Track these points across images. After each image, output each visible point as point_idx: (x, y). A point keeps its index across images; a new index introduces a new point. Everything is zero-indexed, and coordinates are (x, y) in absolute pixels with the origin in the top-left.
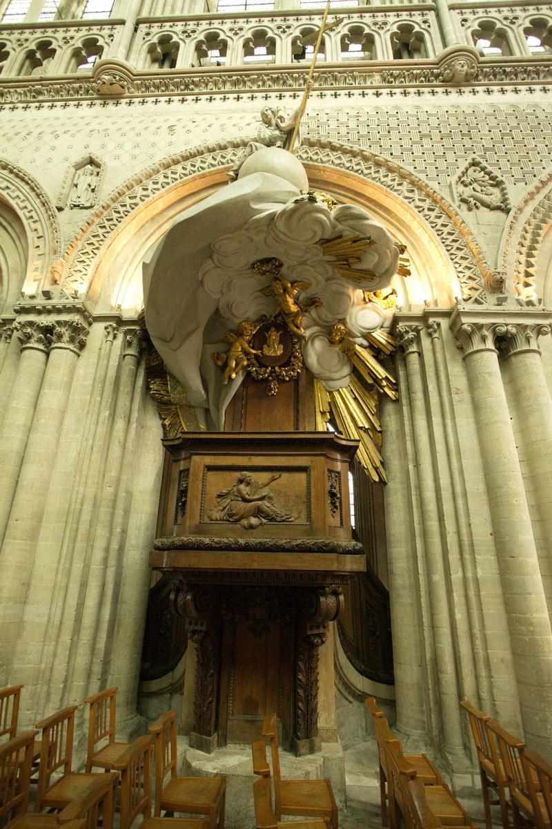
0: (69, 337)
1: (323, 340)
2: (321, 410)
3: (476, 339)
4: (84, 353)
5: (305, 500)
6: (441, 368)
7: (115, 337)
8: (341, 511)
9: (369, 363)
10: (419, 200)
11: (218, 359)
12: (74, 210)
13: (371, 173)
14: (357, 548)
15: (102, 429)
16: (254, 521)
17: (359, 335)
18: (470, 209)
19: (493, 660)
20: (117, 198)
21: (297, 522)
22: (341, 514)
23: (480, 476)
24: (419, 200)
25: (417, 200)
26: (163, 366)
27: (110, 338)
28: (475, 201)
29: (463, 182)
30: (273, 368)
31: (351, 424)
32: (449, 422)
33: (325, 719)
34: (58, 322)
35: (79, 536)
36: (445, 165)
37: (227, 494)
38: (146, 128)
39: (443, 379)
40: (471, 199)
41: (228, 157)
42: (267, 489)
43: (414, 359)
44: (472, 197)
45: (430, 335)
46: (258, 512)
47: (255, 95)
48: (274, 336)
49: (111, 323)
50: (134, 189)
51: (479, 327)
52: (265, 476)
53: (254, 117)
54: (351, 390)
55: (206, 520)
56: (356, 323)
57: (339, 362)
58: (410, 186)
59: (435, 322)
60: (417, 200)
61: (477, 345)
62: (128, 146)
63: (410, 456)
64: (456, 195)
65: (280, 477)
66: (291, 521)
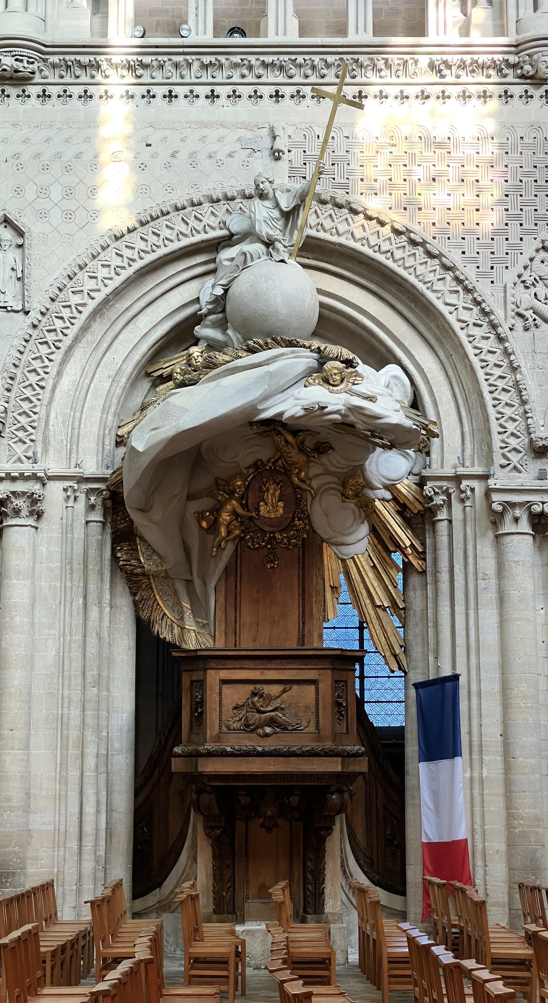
0: (29, 512)
2: (332, 584)
3: (508, 518)
4: (42, 525)
5: (313, 710)
6: (470, 548)
7: (75, 498)
8: (347, 718)
9: (391, 526)
10: (464, 308)
11: (203, 518)
13: (404, 258)
14: (360, 752)
15: (78, 620)
16: (268, 730)
17: (382, 487)
18: (526, 329)
19: (489, 852)
21: (307, 730)
22: (347, 721)
23: (497, 675)
24: (464, 308)
25: (461, 309)
26: (133, 528)
27: (71, 503)
28: (535, 316)
29: (523, 282)
31: (368, 601)
32: (472, 613)
33: (332, 905)
34: (13, 493)
35: (71, 743)
36: (505, 248)
37: (243, 706)
38: (78, 156)
39: (471, 560)
40: (529, 314)
41: (205, 220)
42: (279, 701)
43: (443, 527)
44: (531, 308)
45: (462, 501)
47: (240, 89)
49: (71, 483)
50: (77, 277)
51: (513, 505)
53: (239, 140)
55: (225, 729)
58: (454, 283)
60: (461, 309)
61: (508, 527)
62: (56, 193)
63: (431, 646)
64: (510, 306)
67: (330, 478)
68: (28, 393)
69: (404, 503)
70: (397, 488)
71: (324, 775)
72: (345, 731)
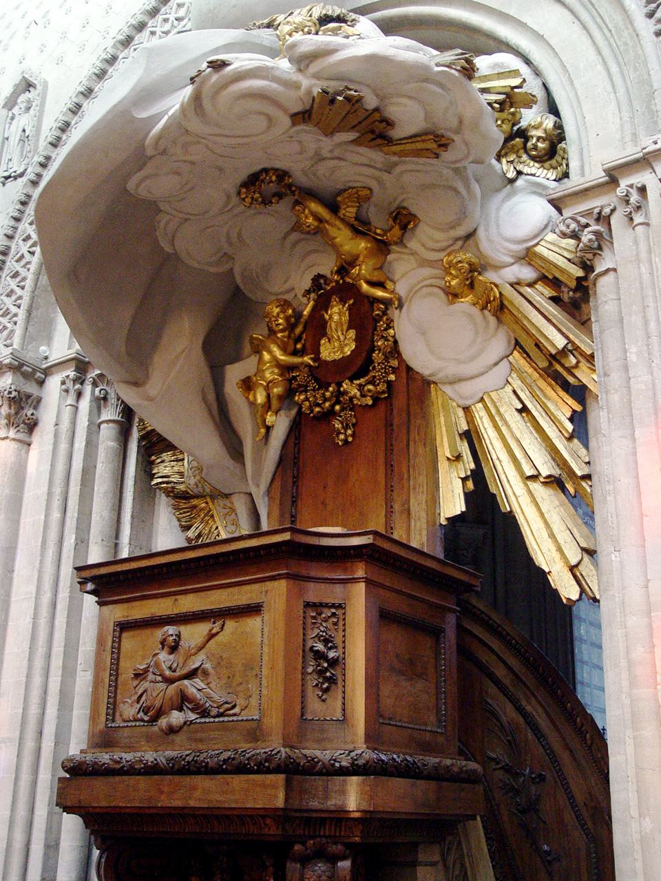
1: (430, 294)
4: (36, 438)
7: (79, 395)
12: (7, 185)
16: (176, 718)
17: (512, 260)
20: (59, 139)
27: (71, 400)
30: (339, 385)
37: (146, 671)
42: (201, 656)
46: (183, 700)
48: (337, 314)
49: (65, 374)
50: (82, 110)
52: (202, 629)
54: (514, 392)
56: (500, 234)
57: (477, 333)
59: (631, 186)
65: (222, 628)
66: (235, 715)
67: (427, 272)
68: (18, 267)
69: (555, 278)
70: (535, 254)
71: (264, 817)
72: (339, 715)
